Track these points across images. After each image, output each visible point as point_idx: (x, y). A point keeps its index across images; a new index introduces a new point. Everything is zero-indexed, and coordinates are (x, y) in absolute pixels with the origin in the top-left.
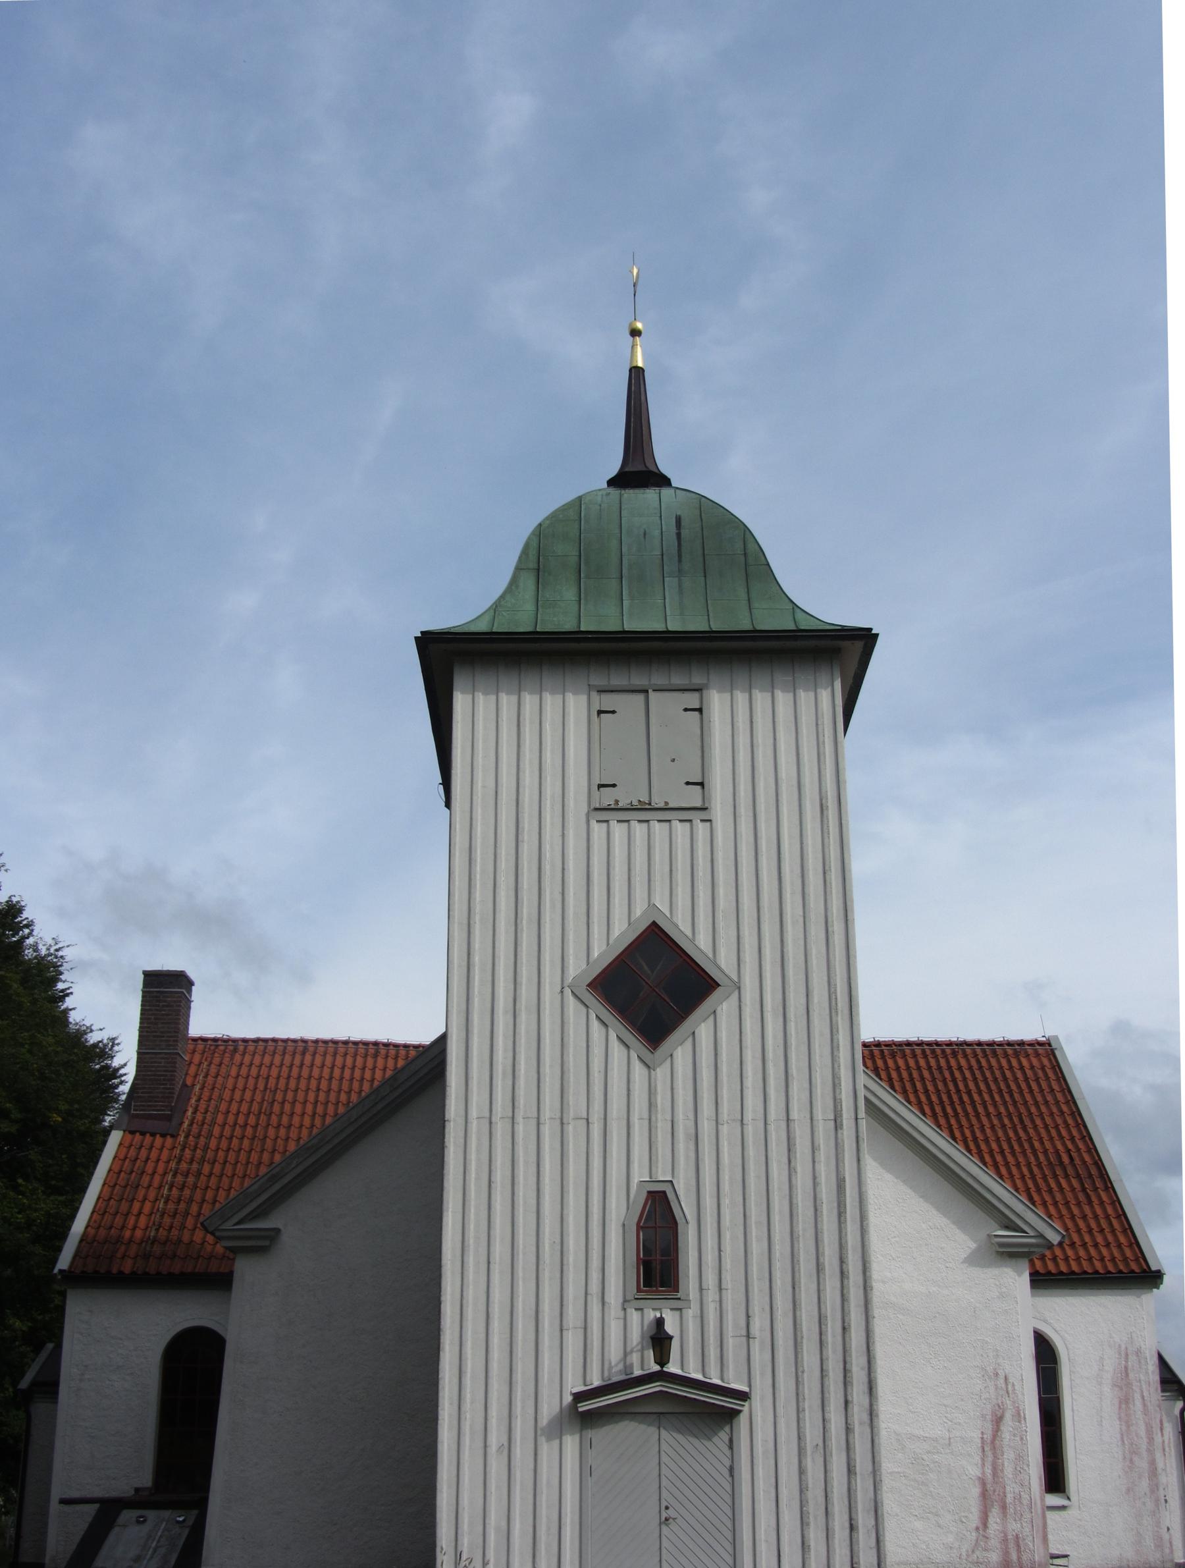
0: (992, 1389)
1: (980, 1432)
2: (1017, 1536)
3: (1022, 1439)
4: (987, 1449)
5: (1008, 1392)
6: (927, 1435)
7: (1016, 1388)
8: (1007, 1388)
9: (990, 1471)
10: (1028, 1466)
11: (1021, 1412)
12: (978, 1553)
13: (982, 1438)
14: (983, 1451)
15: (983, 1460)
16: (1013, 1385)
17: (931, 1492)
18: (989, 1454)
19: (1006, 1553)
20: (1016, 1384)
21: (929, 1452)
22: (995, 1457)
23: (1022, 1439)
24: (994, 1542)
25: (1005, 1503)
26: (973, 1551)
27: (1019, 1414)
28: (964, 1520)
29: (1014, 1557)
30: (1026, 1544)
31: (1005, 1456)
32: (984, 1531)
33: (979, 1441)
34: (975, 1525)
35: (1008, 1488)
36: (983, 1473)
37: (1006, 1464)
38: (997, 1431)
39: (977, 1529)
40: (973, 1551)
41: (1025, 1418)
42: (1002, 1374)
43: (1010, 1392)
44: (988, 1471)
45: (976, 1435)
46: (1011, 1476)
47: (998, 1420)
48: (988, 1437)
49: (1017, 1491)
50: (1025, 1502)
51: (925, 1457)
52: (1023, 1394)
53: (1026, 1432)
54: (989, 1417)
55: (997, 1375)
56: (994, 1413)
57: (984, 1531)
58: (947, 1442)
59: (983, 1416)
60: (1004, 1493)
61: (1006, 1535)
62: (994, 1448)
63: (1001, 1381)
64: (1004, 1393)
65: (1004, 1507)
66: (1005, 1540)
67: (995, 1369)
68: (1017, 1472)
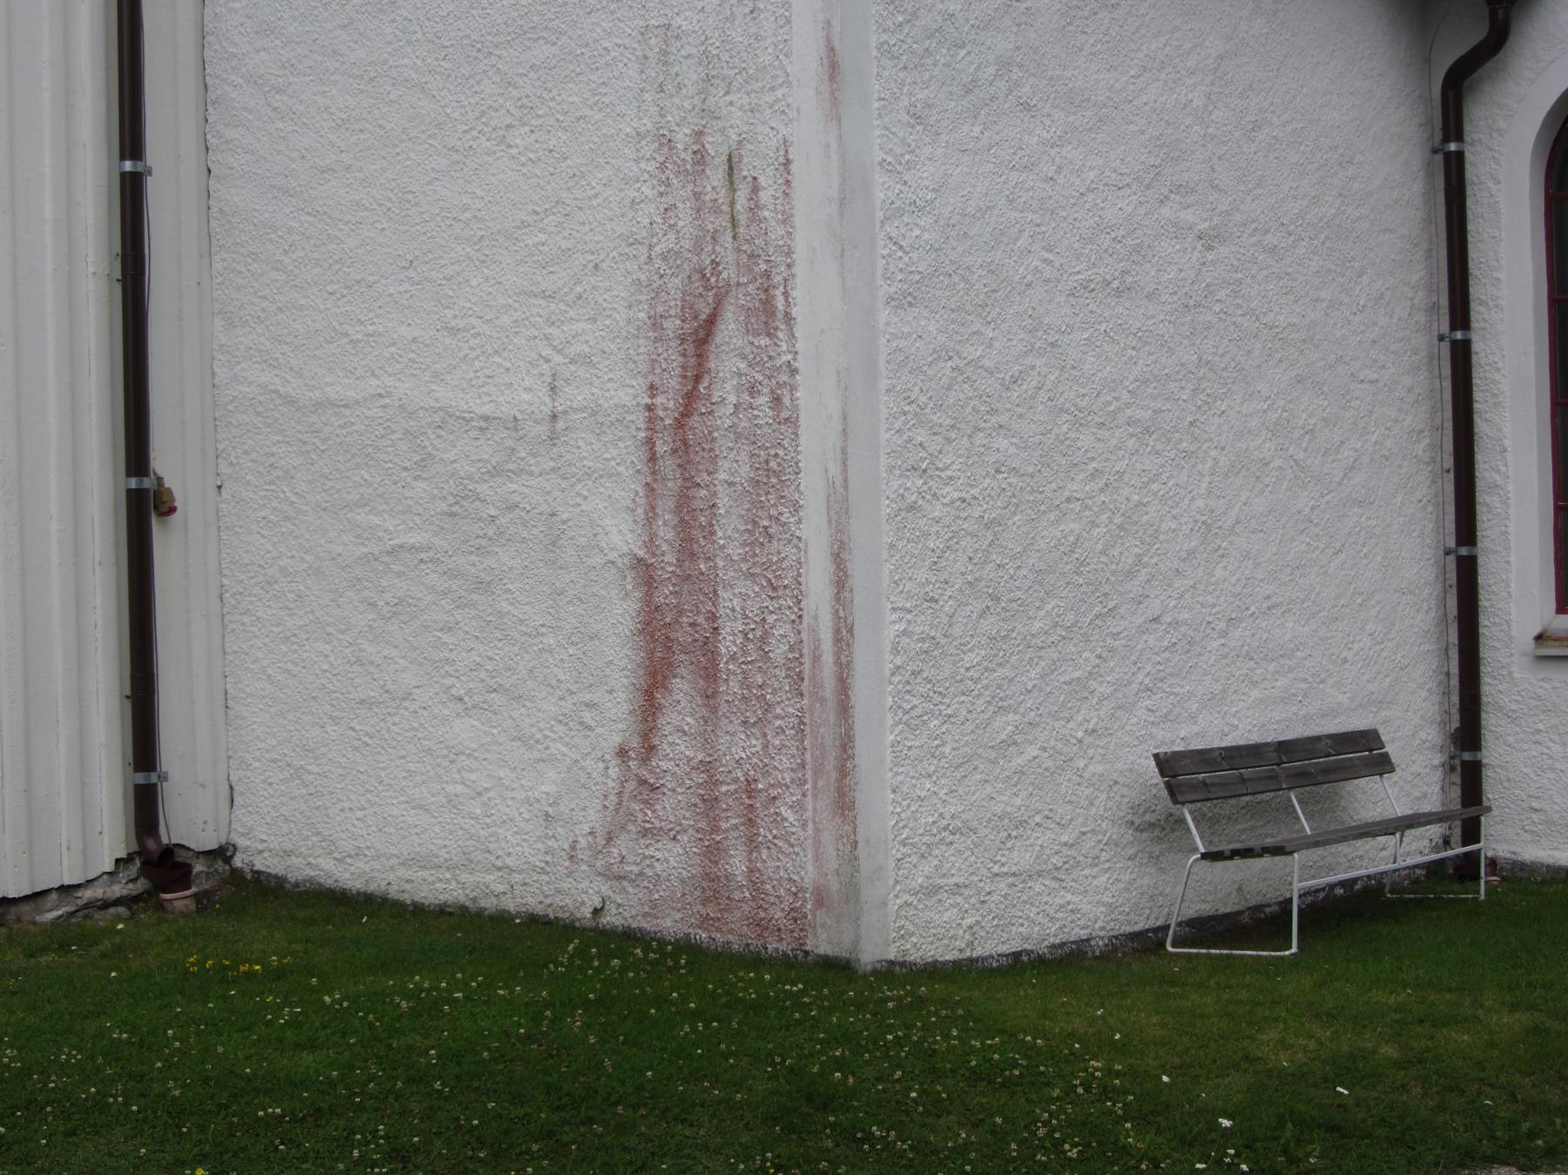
0: (685, 212)
1: (640, 384)
2: (750, 788)
3: (777, 400)
4: (661, 448)
5: (734, 223)
6: (487, 409)
7: (765, 197)
8: (732, 204)
9: (670, 535)
10: (796, 508)
11: (778, 292)
12: (623, 844)
13: (650, 408)
14: (653, 458)
15: (650, 490)
16: (755, 189)
17: (500, 614)
18: (668, 465)
19: (714, 852)
20: (762, 180)
21: (496, 471)
22: (689, 483)
23: (777, 400)
24: (673, 806)
25: (713, 655)
26: (609, 839)
27: (768, 306)
28: (588, 717)
29: (737, 864)
30: (778, 819)
31: (722, 476)
32: (645, 761)
33: (640, 419)
34: (617, 739)
35: (729, 600)
36: (651, 543)
37: (723, 502)
38: (697, 379)
39: (622, 753)
40: (609, 839)
41: (788, 318)
42: (716, 146)
43: (742, 218)
44: (666, 533)
45: (626, 393)
46: (735, 551)
47: (702, 336)
48: (668, 403)
49: (753, 609)
50: (779, 652)
51: (482, 488)
52: (787, 220)
53: (794, 372)
54: (672, 325)
55: (700, 157)
56: (687, 306)
57: (645, 761)
58: (543, 430)
59: (656, 322)
60: (713, 617)
61: (712, 783)
62: (683, 449)
63: (716, 176)
64: (724, 221)
65: (710, 674)
66: (710, 802)
67: (699, 134)
68: (759, 534)
